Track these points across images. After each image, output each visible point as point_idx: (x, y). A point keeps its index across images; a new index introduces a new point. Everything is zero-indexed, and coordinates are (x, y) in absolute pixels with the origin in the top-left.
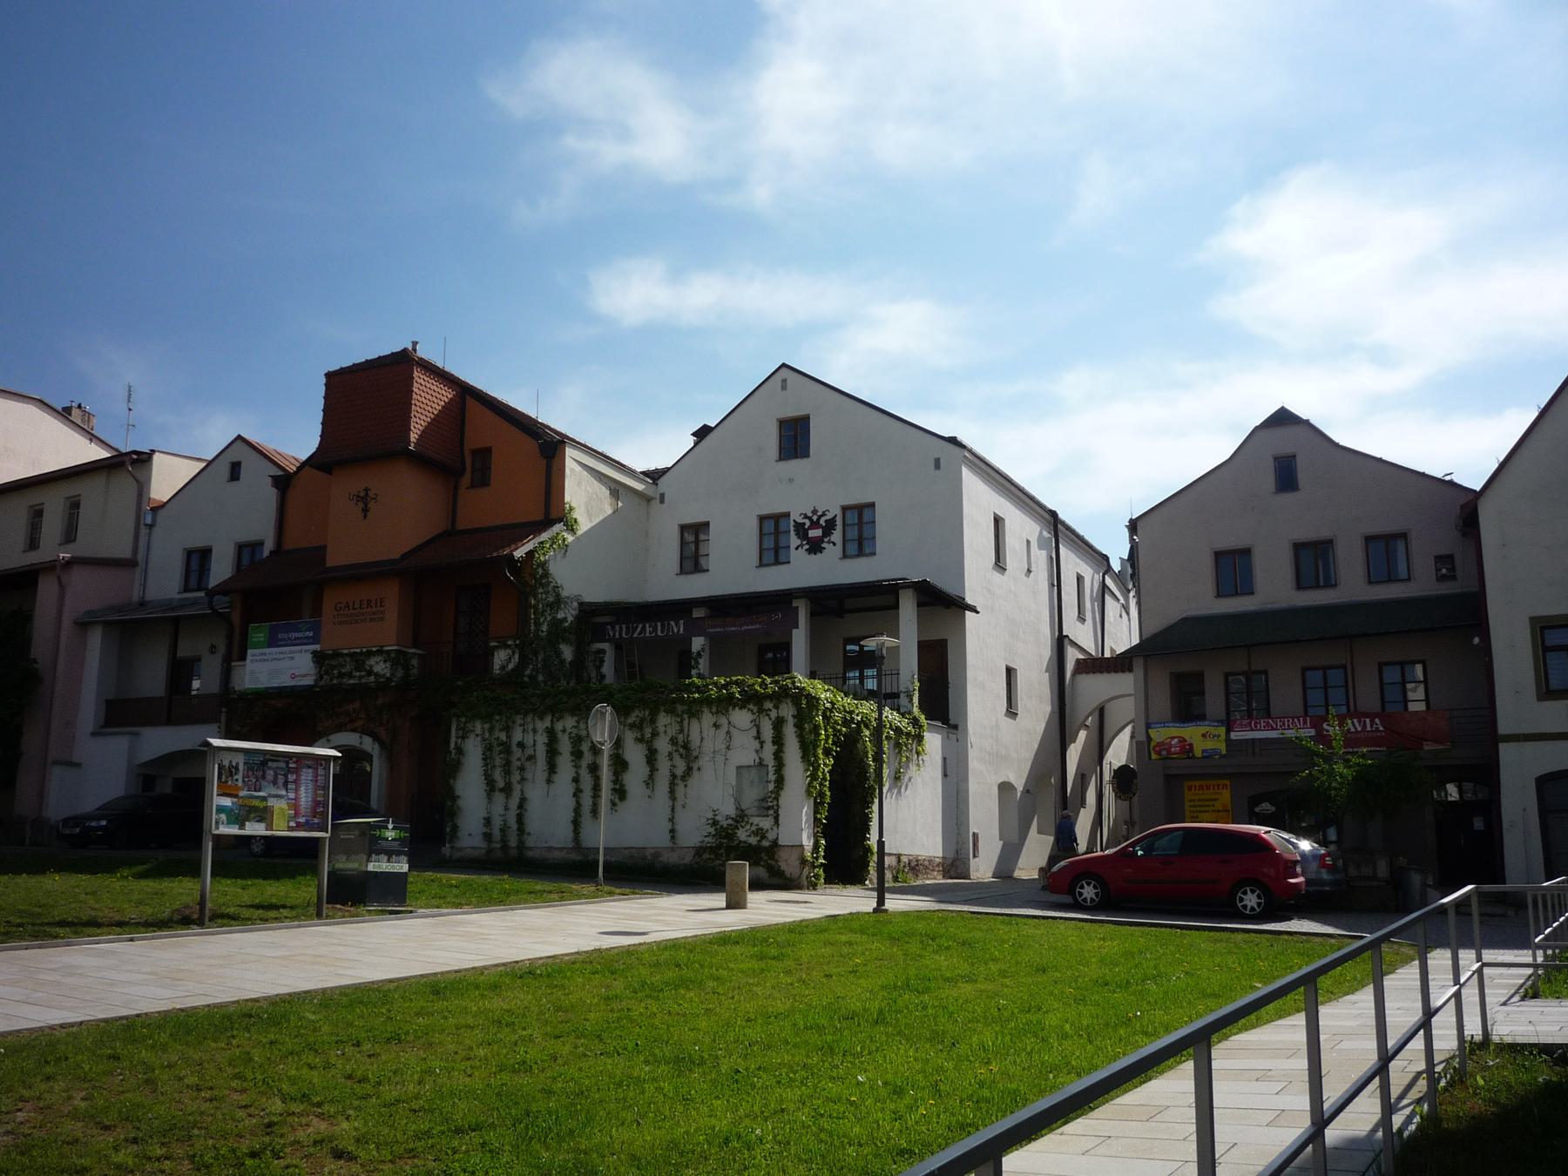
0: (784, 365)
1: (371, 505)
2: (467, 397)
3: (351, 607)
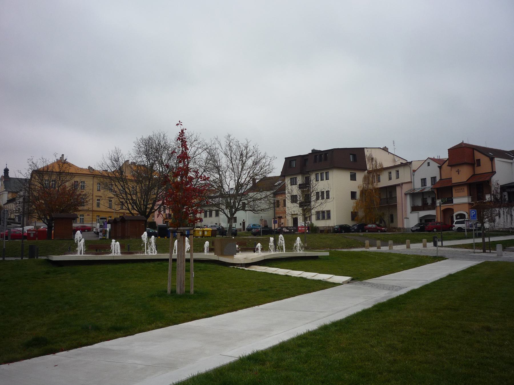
1: (460, 172)
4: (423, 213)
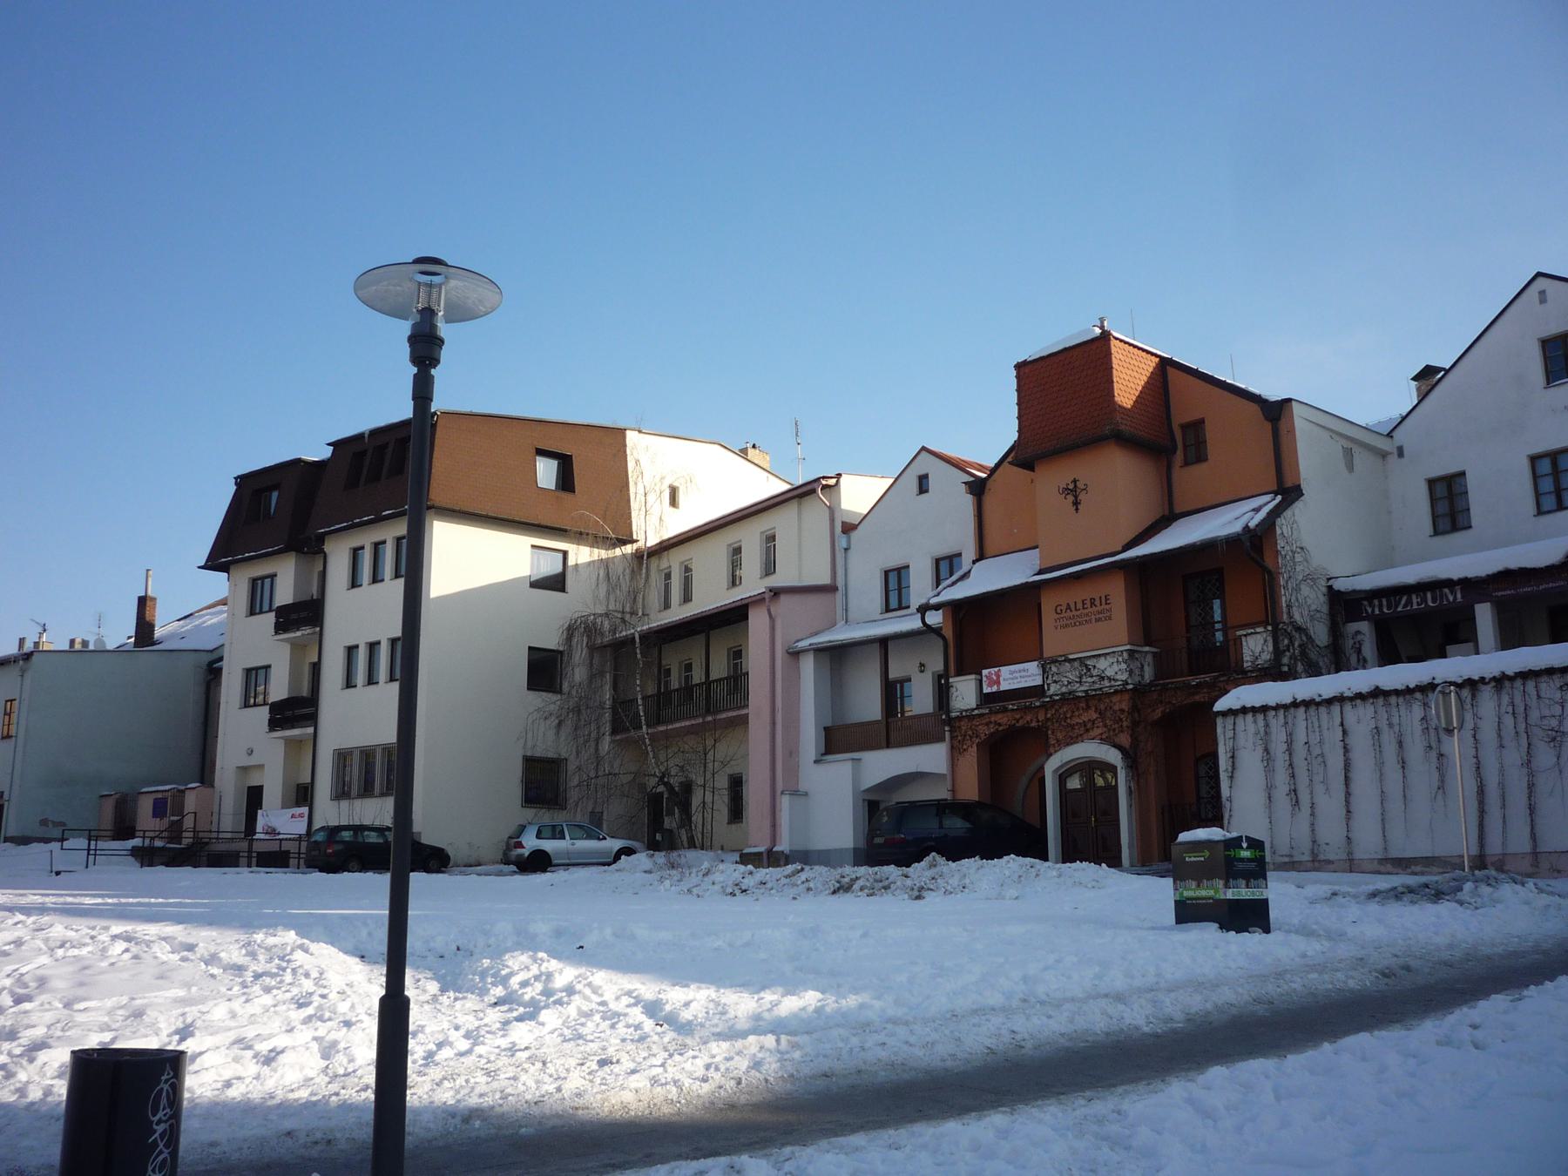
0: (1539, 275)
1: (1082, 497)
2: (1168, 367)
3: (1073, 609)
4: (883, 764)
